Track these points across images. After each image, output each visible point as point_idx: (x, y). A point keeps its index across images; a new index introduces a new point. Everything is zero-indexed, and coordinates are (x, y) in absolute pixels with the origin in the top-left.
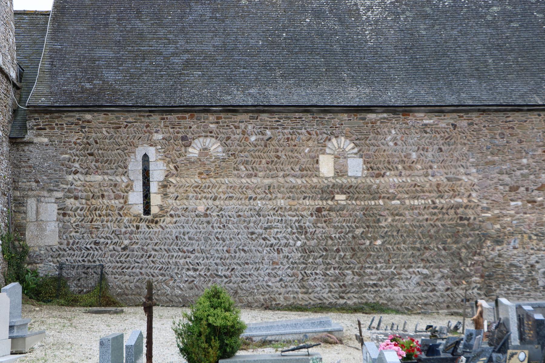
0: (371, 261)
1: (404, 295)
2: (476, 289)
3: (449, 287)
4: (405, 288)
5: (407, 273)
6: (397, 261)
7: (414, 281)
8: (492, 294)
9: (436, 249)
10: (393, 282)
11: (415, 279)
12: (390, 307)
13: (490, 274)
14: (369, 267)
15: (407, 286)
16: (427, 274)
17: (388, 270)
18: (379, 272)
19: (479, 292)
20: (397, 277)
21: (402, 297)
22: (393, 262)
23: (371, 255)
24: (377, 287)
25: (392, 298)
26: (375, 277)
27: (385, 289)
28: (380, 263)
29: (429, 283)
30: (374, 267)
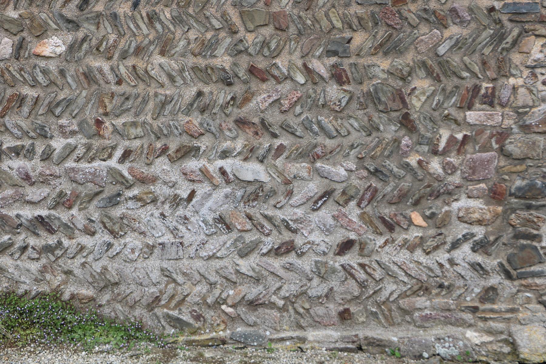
0: (23, 124)
1: (165, 265)
2: (466, 248)
3: (353, 236)
4: (168, 238)
5: (175, 176)
6: (134, 124)
7: (204, 211)
8: (536, 268)
9: (301, 79)
10: (117, 212)
11: (210, 203)
12: (106, 311)
13: (532, 186)
14: (17, 152)
15: (174, 231)
16: (261, 185)
17: (96, 164)
18: (57, 170)
19: (479, 258)
20: (135, 191)
21: (155, 276)
22: (116, 131)
23: (21, 100)
24: (51, 231)
25: (113, 276)
26: (45, 191)
27: (86, 240)
28: (63, 132)
29: (269, 219)
30: (40, 149)
